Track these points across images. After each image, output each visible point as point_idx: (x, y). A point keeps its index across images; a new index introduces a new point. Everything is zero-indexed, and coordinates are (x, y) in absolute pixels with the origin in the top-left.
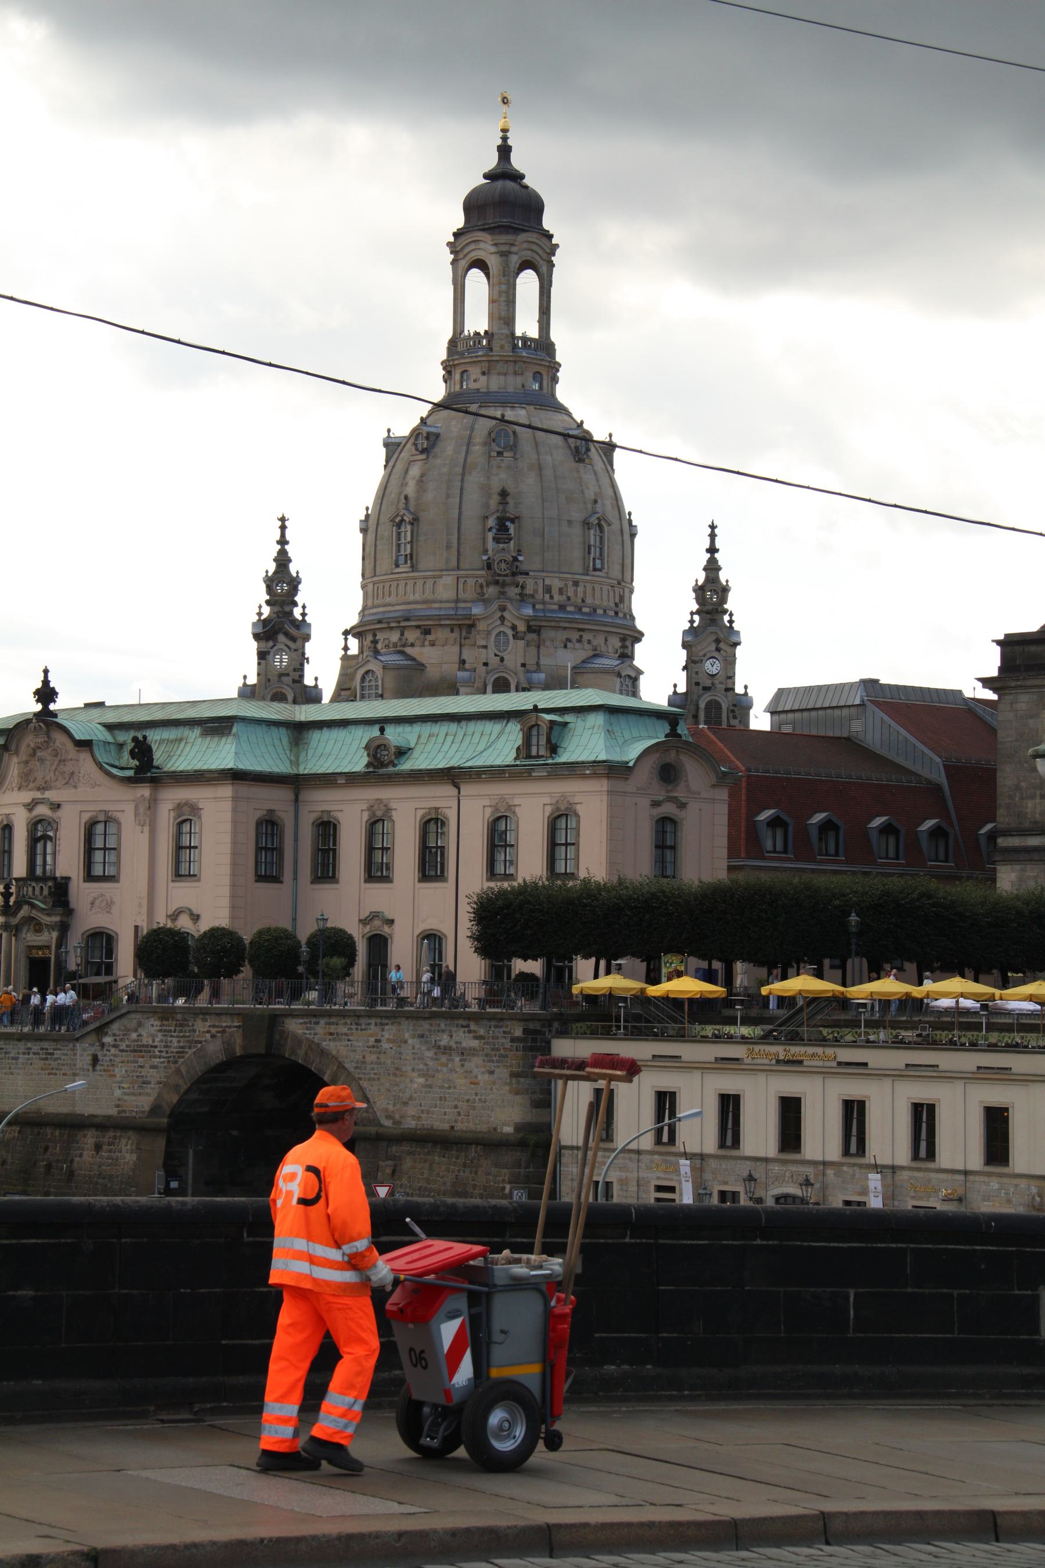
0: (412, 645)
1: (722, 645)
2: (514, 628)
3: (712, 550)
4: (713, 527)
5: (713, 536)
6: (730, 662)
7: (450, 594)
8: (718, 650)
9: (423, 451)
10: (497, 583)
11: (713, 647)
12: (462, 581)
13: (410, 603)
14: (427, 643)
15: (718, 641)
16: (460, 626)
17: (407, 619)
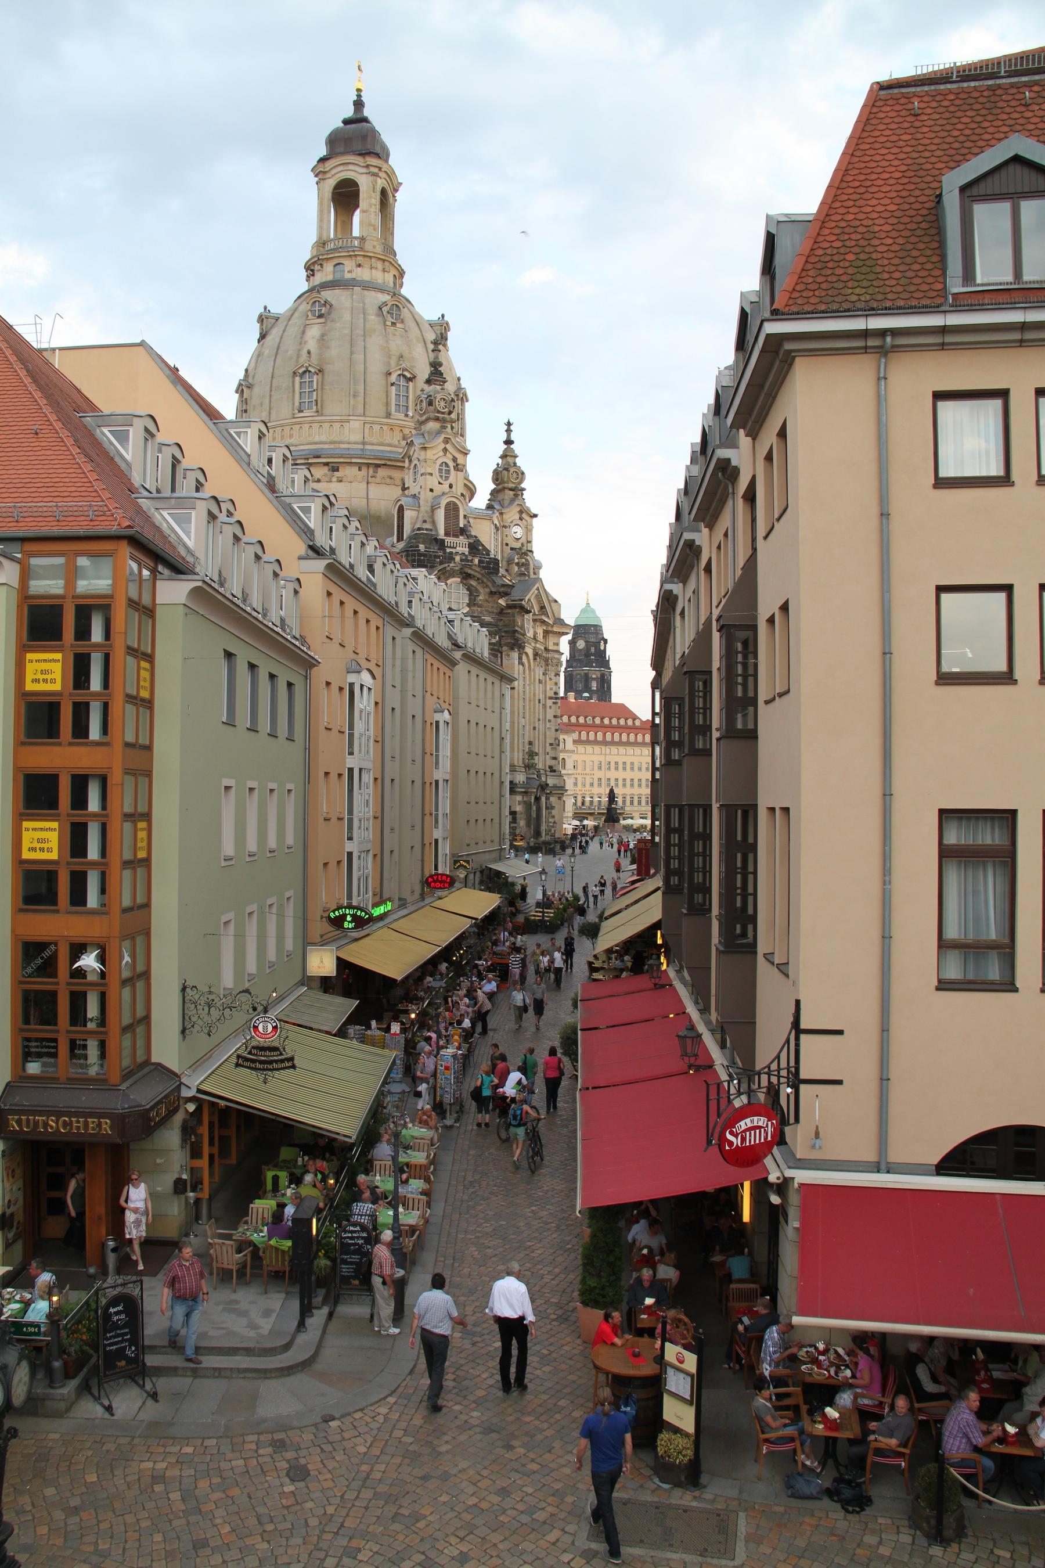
0: (319, 481)
1: (524, 516)
2: (455, 460)
3: (509, 442)
4: (509, 424)
5: (509, 431)
6: (528, 530)
7: (356, 437)
8: (521, 519)
9: (321, 316)
10: (437, 419)
11: (517, 516)
12: (367, 426)
13: (316, 443)
14: (334, 479)
15: (521, 512)
16: (368, 465)
17: (318, 457)
